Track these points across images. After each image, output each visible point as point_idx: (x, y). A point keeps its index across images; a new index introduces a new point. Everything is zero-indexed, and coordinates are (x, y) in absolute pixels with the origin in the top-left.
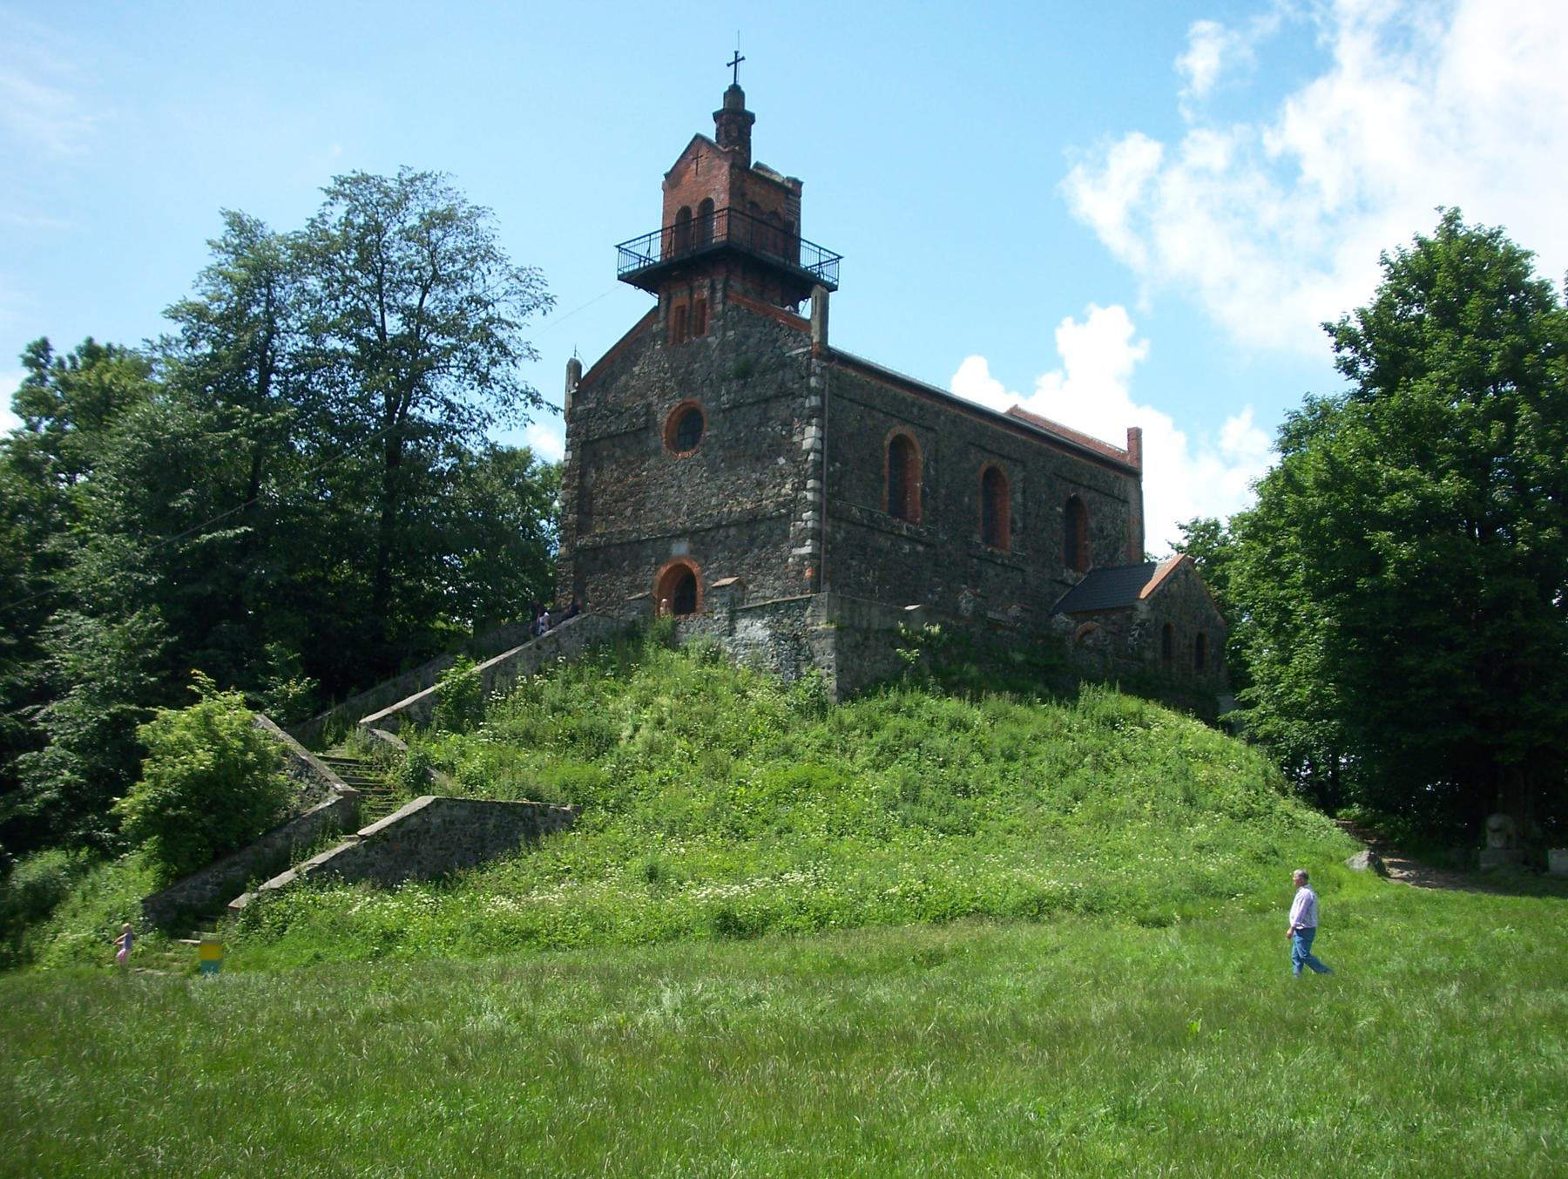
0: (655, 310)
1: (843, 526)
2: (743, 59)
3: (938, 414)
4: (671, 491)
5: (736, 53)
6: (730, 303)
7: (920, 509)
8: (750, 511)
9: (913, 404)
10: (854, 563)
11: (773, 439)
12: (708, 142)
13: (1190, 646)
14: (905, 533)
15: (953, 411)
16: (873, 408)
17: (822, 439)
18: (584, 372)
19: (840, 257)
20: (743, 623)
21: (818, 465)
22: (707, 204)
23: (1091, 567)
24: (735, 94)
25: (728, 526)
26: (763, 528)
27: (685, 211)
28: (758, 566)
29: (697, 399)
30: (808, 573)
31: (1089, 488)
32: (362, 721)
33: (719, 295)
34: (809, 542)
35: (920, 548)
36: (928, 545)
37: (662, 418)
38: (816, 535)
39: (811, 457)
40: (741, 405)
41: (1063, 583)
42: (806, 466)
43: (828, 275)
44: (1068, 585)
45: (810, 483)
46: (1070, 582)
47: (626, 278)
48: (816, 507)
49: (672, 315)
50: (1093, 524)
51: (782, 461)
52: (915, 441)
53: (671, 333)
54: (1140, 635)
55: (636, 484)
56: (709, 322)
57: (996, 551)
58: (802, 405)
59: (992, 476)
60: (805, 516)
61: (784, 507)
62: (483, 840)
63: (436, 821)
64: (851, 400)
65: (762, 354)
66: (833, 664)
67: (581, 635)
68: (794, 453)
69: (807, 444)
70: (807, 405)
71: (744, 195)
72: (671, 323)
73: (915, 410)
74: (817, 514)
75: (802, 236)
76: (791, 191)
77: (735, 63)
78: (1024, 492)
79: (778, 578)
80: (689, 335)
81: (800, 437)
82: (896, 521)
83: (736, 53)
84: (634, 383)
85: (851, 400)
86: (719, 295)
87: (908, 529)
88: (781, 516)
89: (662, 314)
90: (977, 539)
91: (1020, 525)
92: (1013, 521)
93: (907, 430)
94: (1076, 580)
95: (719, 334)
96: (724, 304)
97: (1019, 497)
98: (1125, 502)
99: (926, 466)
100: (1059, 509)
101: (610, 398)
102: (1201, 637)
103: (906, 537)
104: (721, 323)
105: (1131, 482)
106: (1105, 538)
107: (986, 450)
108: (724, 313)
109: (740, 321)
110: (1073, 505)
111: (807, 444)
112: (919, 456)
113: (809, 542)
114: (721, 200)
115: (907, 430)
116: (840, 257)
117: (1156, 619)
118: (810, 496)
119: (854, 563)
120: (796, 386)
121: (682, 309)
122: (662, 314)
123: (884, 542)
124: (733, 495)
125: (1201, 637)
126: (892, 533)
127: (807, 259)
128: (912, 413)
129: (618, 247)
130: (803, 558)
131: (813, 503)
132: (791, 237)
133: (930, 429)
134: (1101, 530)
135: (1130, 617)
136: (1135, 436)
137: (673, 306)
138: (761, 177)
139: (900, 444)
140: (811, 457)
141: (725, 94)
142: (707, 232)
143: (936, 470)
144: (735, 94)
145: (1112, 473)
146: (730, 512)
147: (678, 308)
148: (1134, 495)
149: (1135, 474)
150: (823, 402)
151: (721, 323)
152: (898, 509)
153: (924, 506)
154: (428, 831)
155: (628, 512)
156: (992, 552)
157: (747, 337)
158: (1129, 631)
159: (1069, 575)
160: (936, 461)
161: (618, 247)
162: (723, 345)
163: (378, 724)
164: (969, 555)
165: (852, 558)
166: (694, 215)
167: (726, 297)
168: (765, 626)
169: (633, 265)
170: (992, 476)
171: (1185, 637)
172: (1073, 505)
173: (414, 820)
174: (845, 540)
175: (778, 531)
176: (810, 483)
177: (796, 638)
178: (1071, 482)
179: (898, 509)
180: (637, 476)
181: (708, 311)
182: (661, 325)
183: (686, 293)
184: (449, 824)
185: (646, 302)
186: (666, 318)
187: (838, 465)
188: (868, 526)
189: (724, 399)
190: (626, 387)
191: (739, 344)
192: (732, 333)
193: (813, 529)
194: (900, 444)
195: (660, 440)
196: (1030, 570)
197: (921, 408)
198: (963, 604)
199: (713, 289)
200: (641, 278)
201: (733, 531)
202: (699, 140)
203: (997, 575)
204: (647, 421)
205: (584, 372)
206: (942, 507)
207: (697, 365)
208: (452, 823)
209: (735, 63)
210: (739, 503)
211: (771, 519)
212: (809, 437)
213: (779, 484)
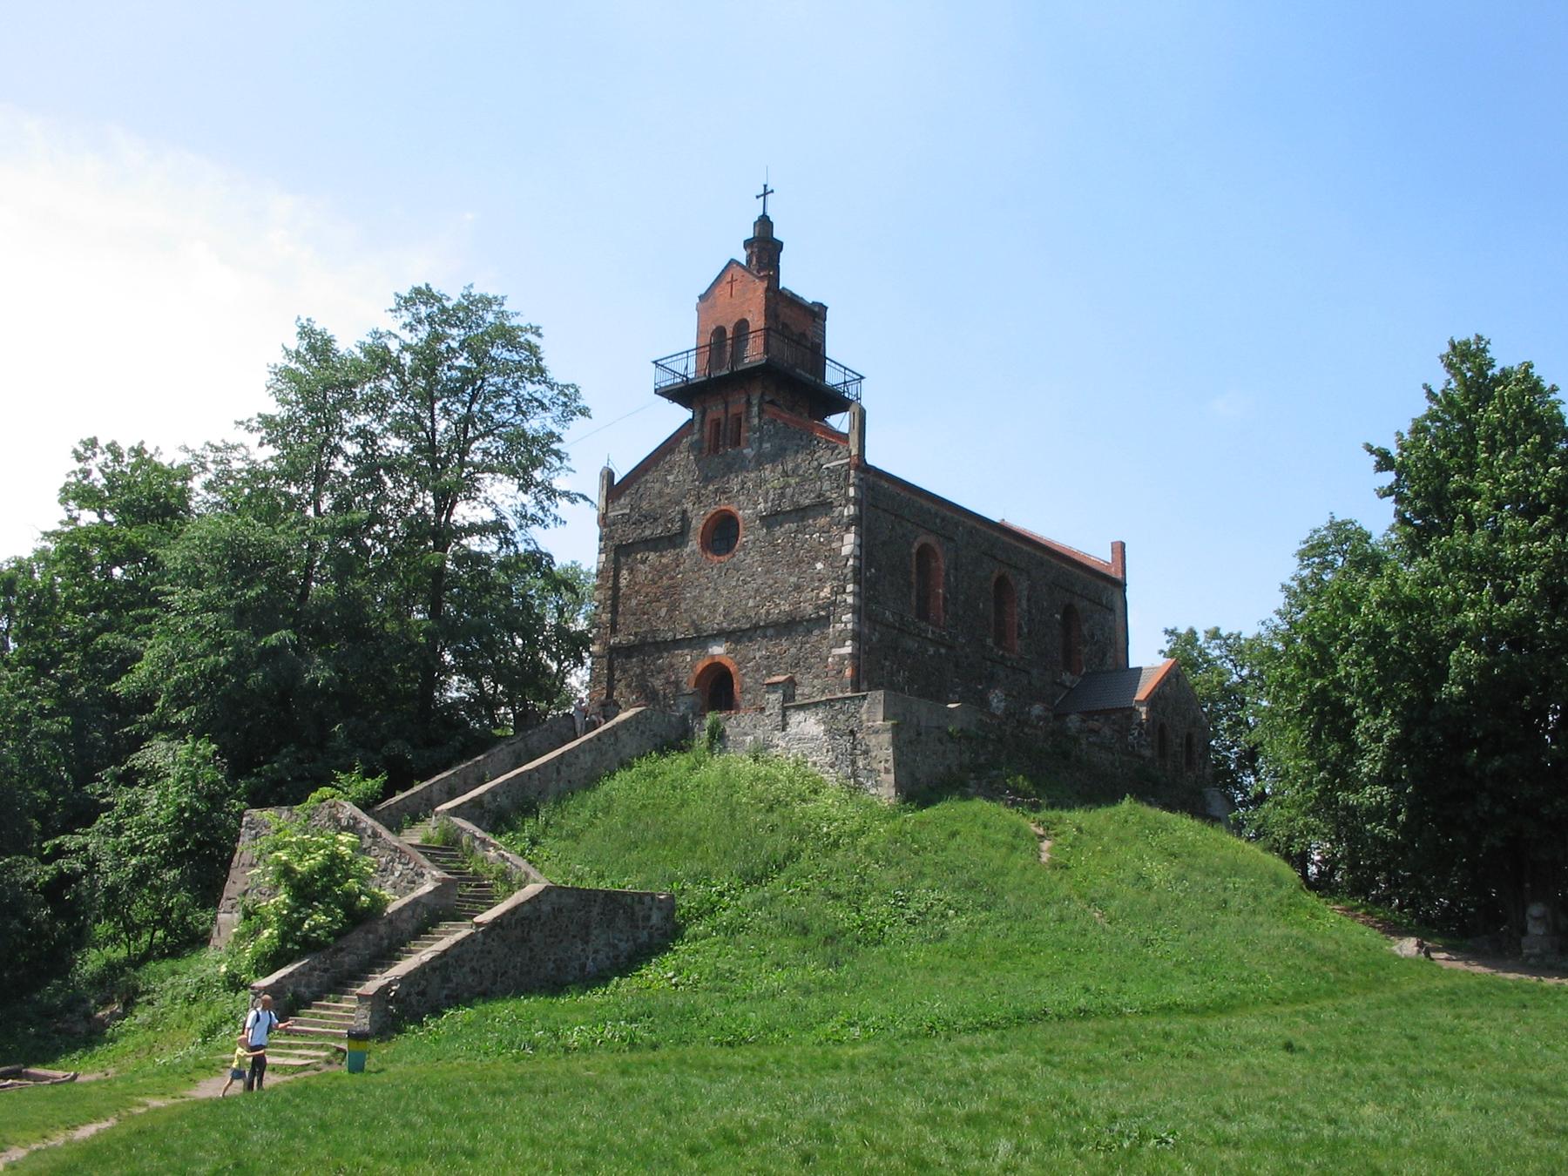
0: (690, 423)
1: (878, 628)
2: (772, 191)
3: (957, 525)
4: (707, 594)
5: (765, 186)
6: (766, 417)
7: (942, 614)
8: (789, 614)
9: (936, 514)
10: (887, 664)
12: (739, 264)
13: (1181, 745)
14: (930, 636)
15: (970, 523)
17: (860, 546)
18: (616, 481)
19: (862, 378)
20: (795, 718)
21: (857, 571)
22: (742, 326)
23: (1084, 670)
24: (764, 223)
27: (720, 332)
28: (797, 665)
29: (733, 508)
30: (848, 672)
31: (1081, 596)
32: (438, 809)
34: (849, 643)
35: (943, 651)
36: (950, 648)
37: (697, 524)
38: (856, 636)
39: (851, 562)
41: (1062, 685)
42: (845, 571)
43: (851, 393)
44: (1066, 687)
45: (850, 588)
46: (1068, 684)
48: (856, 610)
49: (707, 429)
50: (1085, 629)
51: (819, 566)
52: (938, 550)
53: (706, 445)
54: (1140, 734)
55: (670, 587)
56: (745, 435)
57: (1007, 655)
58: (841, 514)
59: (1001, 583)
61: (823, 609)
62: (588, 927)
63: (546, 908)
64: (885, 510)
66: (891, 758)
67: (637, 728)
68: (833, 557)
70: (846, 514)
71: (777, 316)
73: (938, 521)
74: (856, 616)
75: (827, 355)
76: (816, 314)
77: (765, 194)
78: (1029, 600)
79: (817, 677)
80: (724, 445)
81: (840, 544)
82: (923, 625)
83: (765, 186)
84: (668, 491)
85: (885, 510)
86: (755, 410)
87: (933, 632)
88: (820, 618)
89: (697, 426)
90: (990, 641)
91: (1026, 630)
92: (1020, 627)
93: (930, 540)
94: (1073, 682)
95: (755, 445)
96: (760, 419)
97: (1024, 604)
98: (1112, 610)
99: (947, 575)
100: (1058, 616)
101: (645, 505)
102: (1189, 737)
103: (930, 640)
105: (1117, 592)
106: (1095, 644)
107: (995, 558)
108: (760, 428)
110: (1069, 612)
112: (941, 563)
113: (849, 643)
114: (757, 321)
115: (930, 540)
116: (862, 378)
117: (1154, 721)
118: (850, 600)
119: (887, 664)
121: (717, 423)
122: (697, 426)
123: (912, 644)
124: (770, 598)
125: (1189, 737)
126: (919, 635)
127: (832, 377)
128: (935, 523)
129: (655, 362)
130: (842, 657)
131: (852, 606)
132: (816, 356)
133: (951, 539)
134: (1092, 636)
135: (1129, 717)
136: (1120, 549)
137: (708, 419)
138: (793, 301)
139: (925, 553)
140: (851, 562)
141: (755, 223)
142: (738, 355)
143: (956, 577)
144: (764, 223)
145: (1102, 584)
146: (768, 613)
147: (713, 420)
148: (1119, 604)
149: (1121, 585)
150: (860, 511)
152: (923, 613)
153: (946, 612)
154: (539, 918)
155: (663, 612)
156: (1003, 656)
158: (1128, 730)
159: (1067, 677)
160: (956, 569)
161: (655, 362)
163: (455, 812)
164: (984, 658)
165: (886, 659)
166: (729, 335)
167: (761, 412)
168: (818, 722)
169: (668, 380)
170: (1001, 583)
171: (1177, 736)
172: (1069, 612)
173: (527, 908)
174: (880, 641)
176: (850, 588)
177: (852, 733)
178: (1067, 590)
179: (923, 613)
180: (672, 578)
181: (743, 424)
182: (696, 437)
183: (721, 407)
184: (557, 911)
185: (680, 415)
186: (701, 430)
187: (873, 570)
188: (899, 629)
189: (761, 506)
190: (660, 495)
192: (768, 445)
193: (853, 630)
194: (925, 553)
195: (694, 544)
196: (1035, 672)
197: (943, 519)
198: (995, 702)
199: (749, 403)
200: (679, 393)
202: (732, 262)
203: (1007, 677)
204: (682, 527)
205: (616, 481)
206: (961, 613)
208: (560, 910)
209: (765, 194)
210: (777, 605)
211: (809, 620)
212: (849, 544)
213: (817, 588)
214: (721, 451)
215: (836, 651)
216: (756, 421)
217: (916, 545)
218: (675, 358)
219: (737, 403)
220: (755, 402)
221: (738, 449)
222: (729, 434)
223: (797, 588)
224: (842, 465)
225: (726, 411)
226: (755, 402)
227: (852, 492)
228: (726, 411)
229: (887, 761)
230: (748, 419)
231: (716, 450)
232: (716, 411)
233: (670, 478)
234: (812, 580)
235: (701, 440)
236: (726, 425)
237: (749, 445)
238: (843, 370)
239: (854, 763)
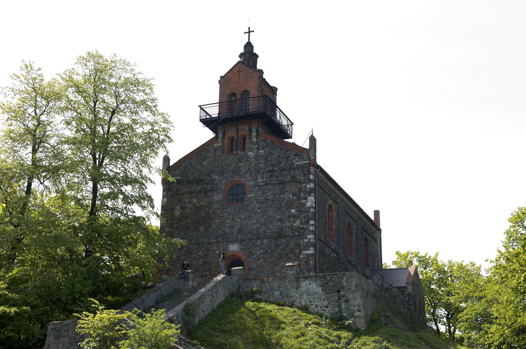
5: (249, 28)
6: (261, 138)
11: (288, 201)
16: (325, 191)
22: (246, 93)
24: (249, 46)
25: (263, 238)
26: (283, 240)
29: (243, 179)
33: (254, 134)
40: (269, 184)
45: (312, 222)
47: (202, 121)
49: (226, 141)
53: (225, 149)
56: (248, 145)
58: (306, 187)
60: (308, 237)
65: (280, 162)
68: (301, 208)
69: (309, 204)
72: (226, 144)
76: (274, 90)
77: (249, 32)
78: (356, 234)
80: (237, 150)
81: (306, 201)
83: (249, 28)
86: (254, 134)
96: (257, 138)
98: (376, 241)
104: (256, 146)
108: (257, 143)
109: (267, 146)
111: (309, 204)
113: (311, 248)
120: (302, 178)
129: (200, 106)
143: (338, 220)
144: (249, 46)
151: (256, 146)
157: (271, 154)
160: (339, 218)
161: (200, 106)
162: (257, 157)
175: (292, 243)
182: (220, 144)
183: (234, 131)
189: (260, 180)
191: (267, 157)
192: (263, 151)
199: (250, 131)
200: (208, 122)
201: (265, 241)
207: (241, 164)
209: (249, 32)
214: (235, 152)
215: (305, 252)
216: (255, 140)
217: (328, 205)
218: (212, 105)
219: (244, 129)
220: (254, 130)
221: (244, 152)
222: (239, 145)
223: (280, 220)
224: (305, 164)
225: (237, 133)
226: (254, 130)
227: (312, 177)
228: (237, 133)
229: (359, 306)
230: (250, 138)
231: (231, 151)
232: (231, 132)
233: (205, 163)
234: (289, 217)
235: (223, 146)
236: (237, 140)
237: (250, 150)
238: (287, 119)
239: (339, 305)
